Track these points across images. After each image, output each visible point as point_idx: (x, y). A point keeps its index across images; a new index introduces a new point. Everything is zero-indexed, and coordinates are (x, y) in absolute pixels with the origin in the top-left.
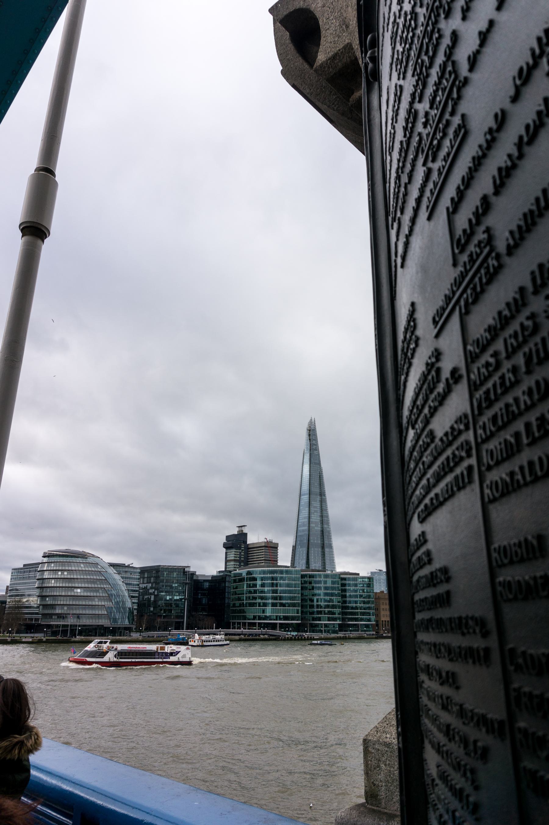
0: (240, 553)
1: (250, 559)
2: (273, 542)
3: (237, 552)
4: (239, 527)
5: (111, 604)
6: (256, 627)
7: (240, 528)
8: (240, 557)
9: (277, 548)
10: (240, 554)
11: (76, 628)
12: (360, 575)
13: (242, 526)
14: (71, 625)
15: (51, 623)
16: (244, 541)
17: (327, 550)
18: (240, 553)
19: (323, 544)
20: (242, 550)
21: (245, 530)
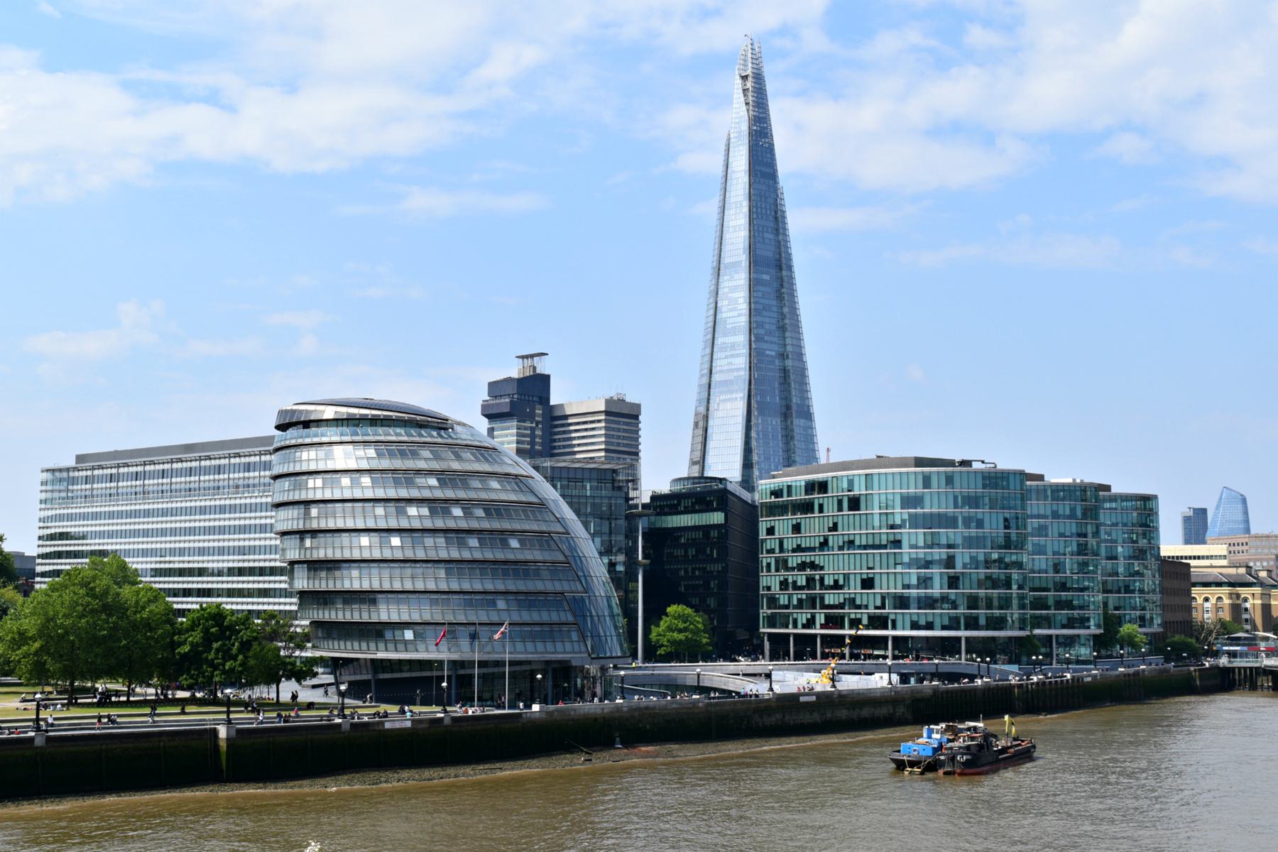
0: (533, 429)
1: (559, 447)
2: (628, 400)
3: (525, 428)
4: (523, 357)
5: (580, 588)
6: (886, 649)
7: (528, 362)
8: (532, 443)
9: (636, 417)
10: (533, 436)
11: (501, 670)
12: (1114, 490)
13: (532, 356)
14: (482, 664)
15: (381, 655)
16: (540, 398)
17: (798, 423)
18: (533, 429)
19: (788, 407)
20: (537, 423)
21: (543, 367)
